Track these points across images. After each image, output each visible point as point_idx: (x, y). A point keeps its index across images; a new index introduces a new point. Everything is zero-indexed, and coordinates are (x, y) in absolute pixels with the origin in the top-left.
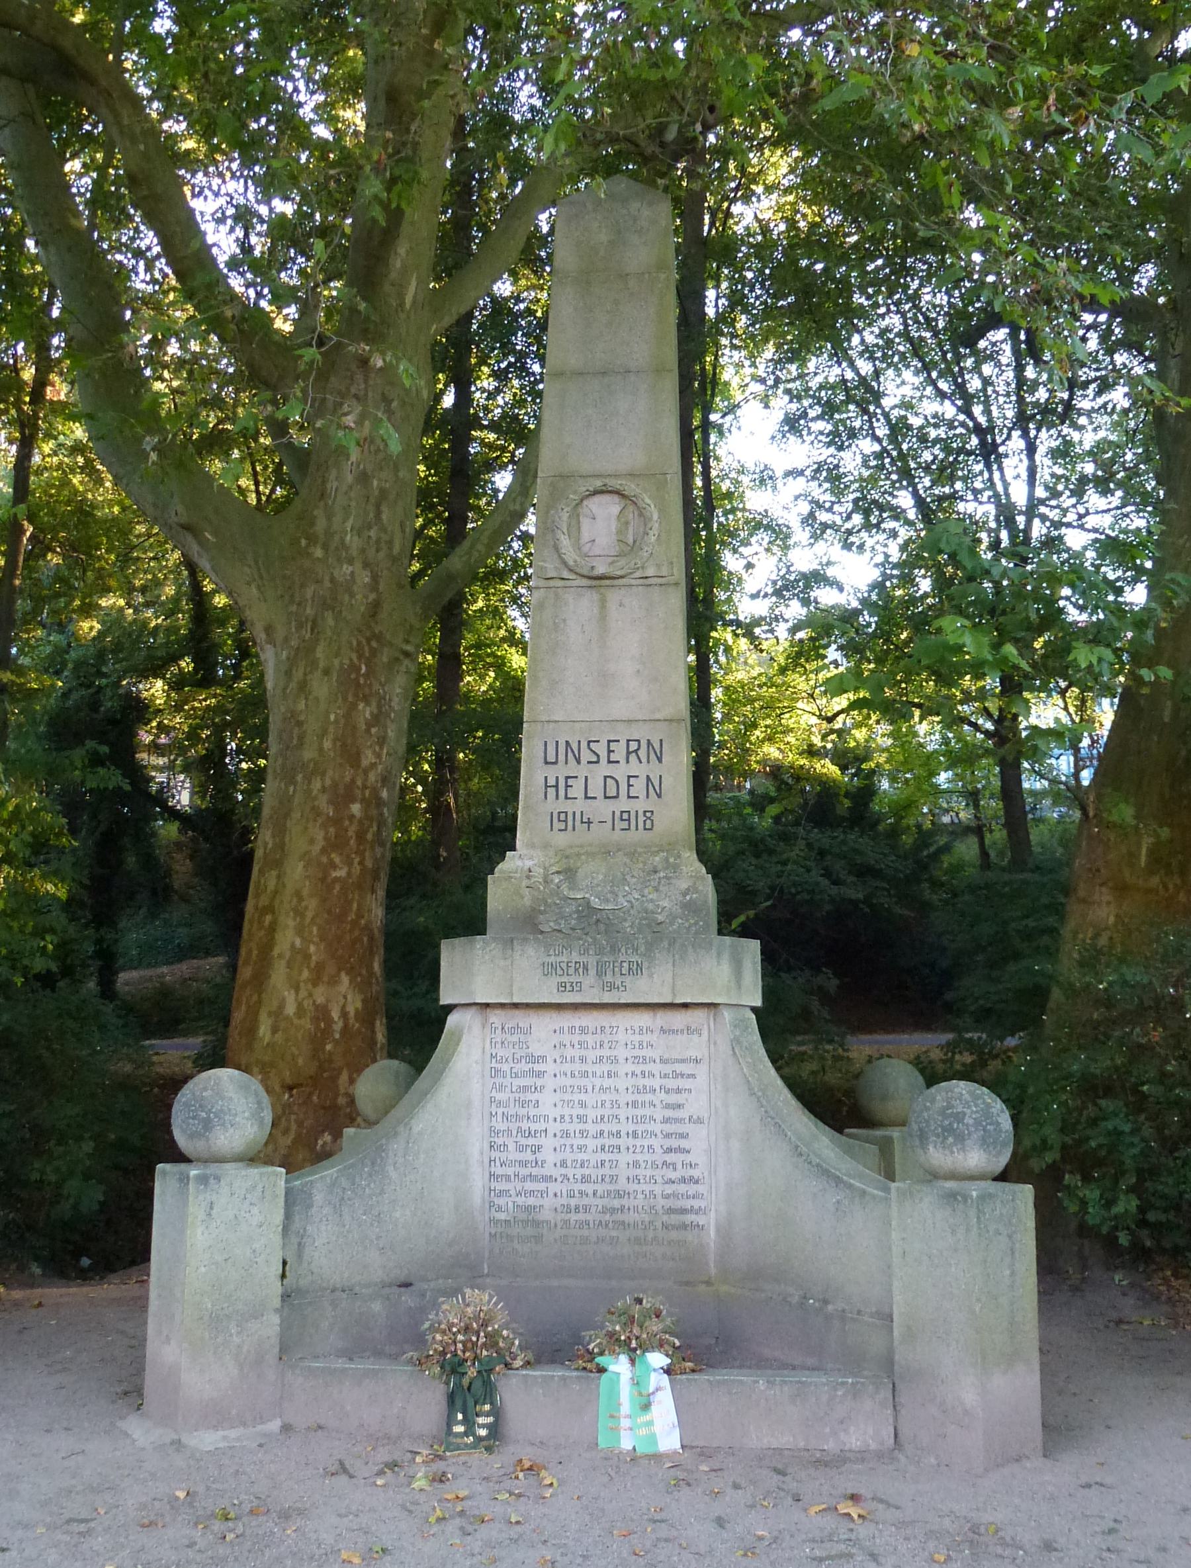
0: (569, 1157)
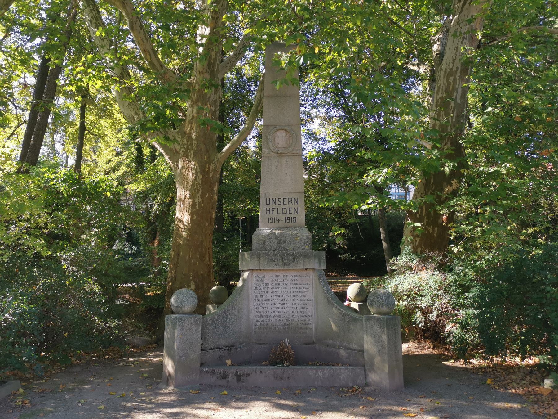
0: (275, 310)
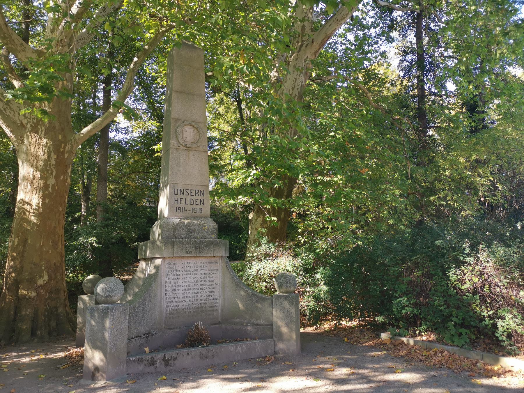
0: (186, 295)
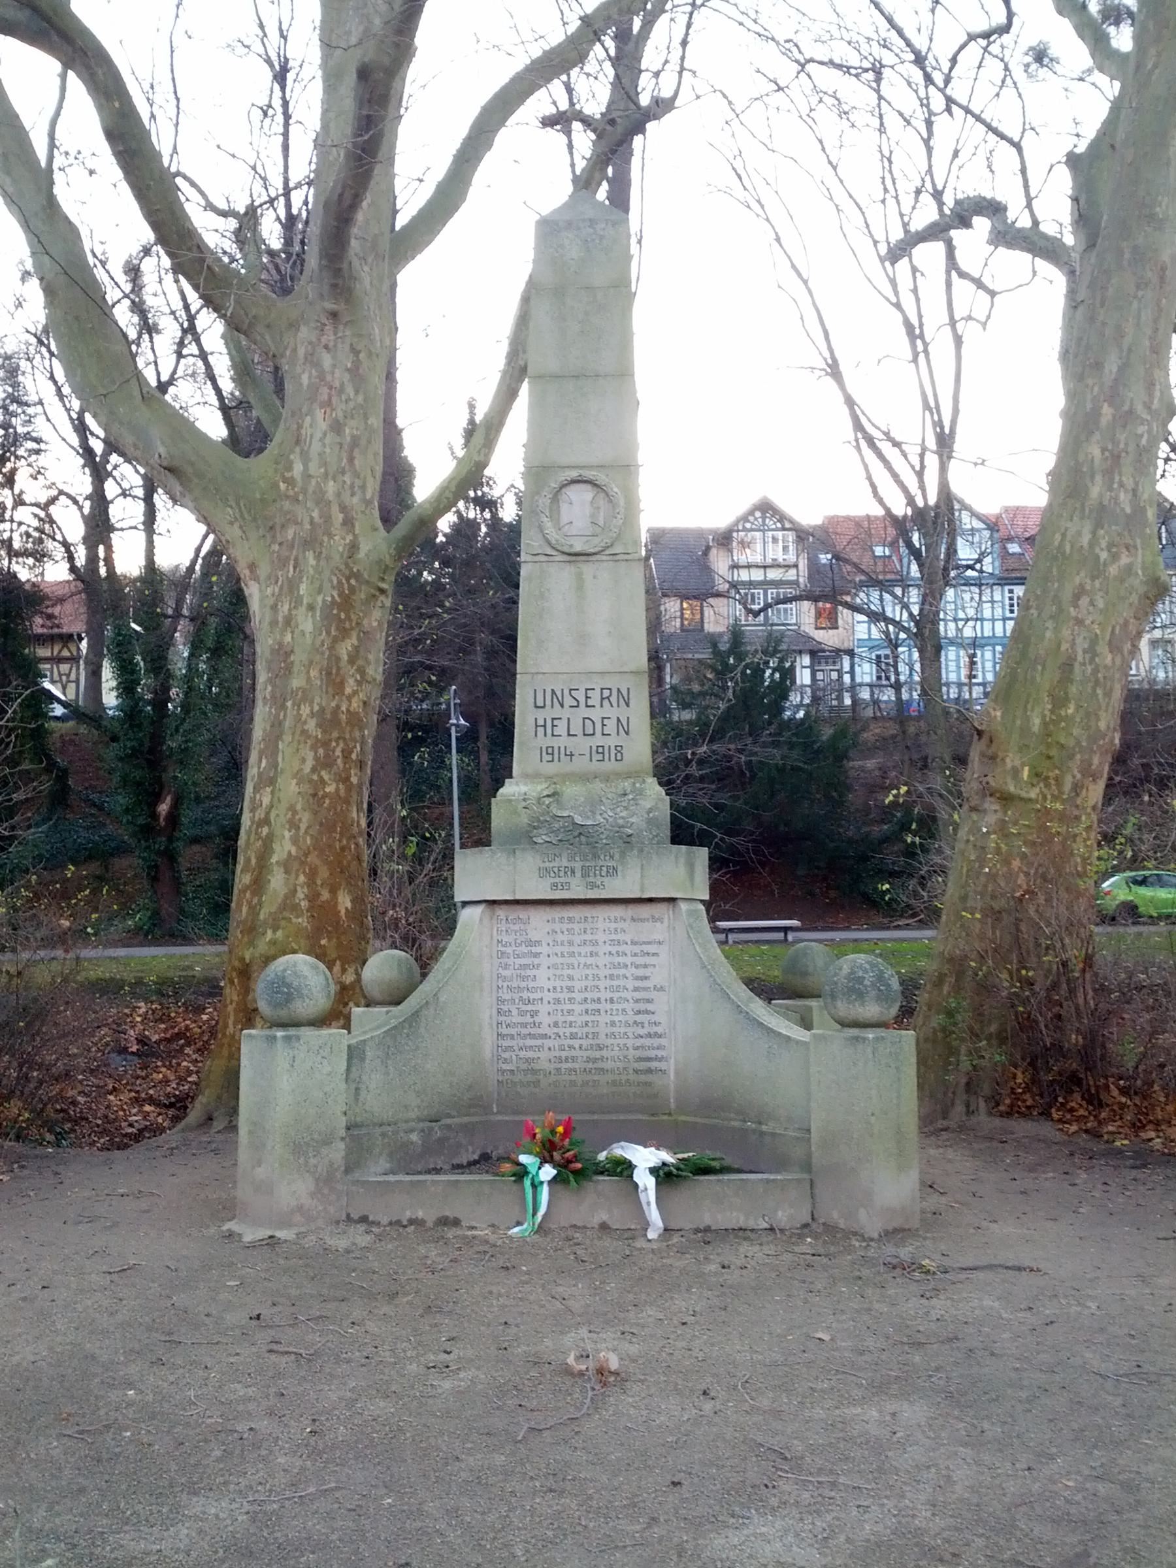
0: (561, 1019)
